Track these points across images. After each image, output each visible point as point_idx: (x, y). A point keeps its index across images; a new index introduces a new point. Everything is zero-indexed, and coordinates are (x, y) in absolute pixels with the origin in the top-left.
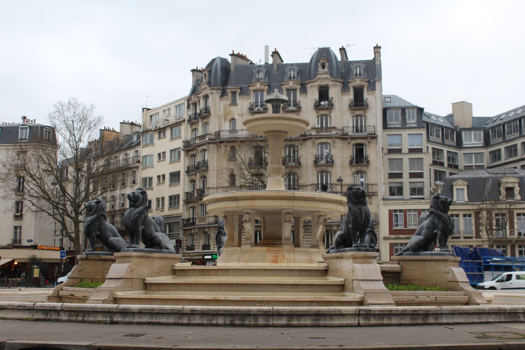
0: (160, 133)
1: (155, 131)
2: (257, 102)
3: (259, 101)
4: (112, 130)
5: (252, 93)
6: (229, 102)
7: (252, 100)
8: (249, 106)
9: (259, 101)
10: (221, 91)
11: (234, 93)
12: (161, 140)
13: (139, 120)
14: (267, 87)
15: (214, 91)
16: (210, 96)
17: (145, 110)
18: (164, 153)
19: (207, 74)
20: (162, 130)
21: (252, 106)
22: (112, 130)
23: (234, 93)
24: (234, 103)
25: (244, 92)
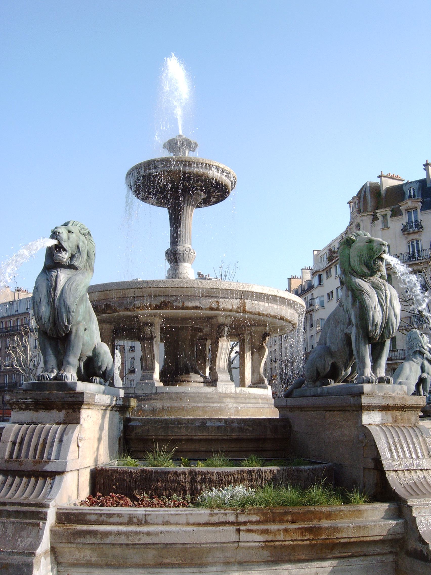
0: (327, 272)
1: (323, 270)
2: (410, 222)
3: (413, 220)
4: (299, 278)
5: (404, 213)
6: (380, 226)
7: (404, 219)
8: (402, 228)
9: (413, 220)
10: (372, 217)
11: (385, 216)
12: (329, 280)
13: (310, 264)
14: (420, 204)
15: (364, 218)
16: (361, 224)
17: (316, 252)
18: (332, 292)
19: (357, 202)
20: (328, 269)
21: (405, 226)
22: (299, 278)
23: (385, 216)
24: (386, 226)
25: (396, 213)
